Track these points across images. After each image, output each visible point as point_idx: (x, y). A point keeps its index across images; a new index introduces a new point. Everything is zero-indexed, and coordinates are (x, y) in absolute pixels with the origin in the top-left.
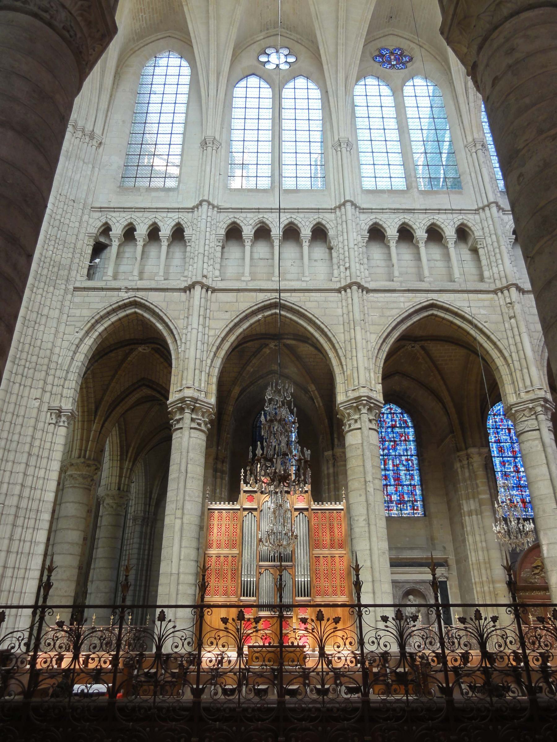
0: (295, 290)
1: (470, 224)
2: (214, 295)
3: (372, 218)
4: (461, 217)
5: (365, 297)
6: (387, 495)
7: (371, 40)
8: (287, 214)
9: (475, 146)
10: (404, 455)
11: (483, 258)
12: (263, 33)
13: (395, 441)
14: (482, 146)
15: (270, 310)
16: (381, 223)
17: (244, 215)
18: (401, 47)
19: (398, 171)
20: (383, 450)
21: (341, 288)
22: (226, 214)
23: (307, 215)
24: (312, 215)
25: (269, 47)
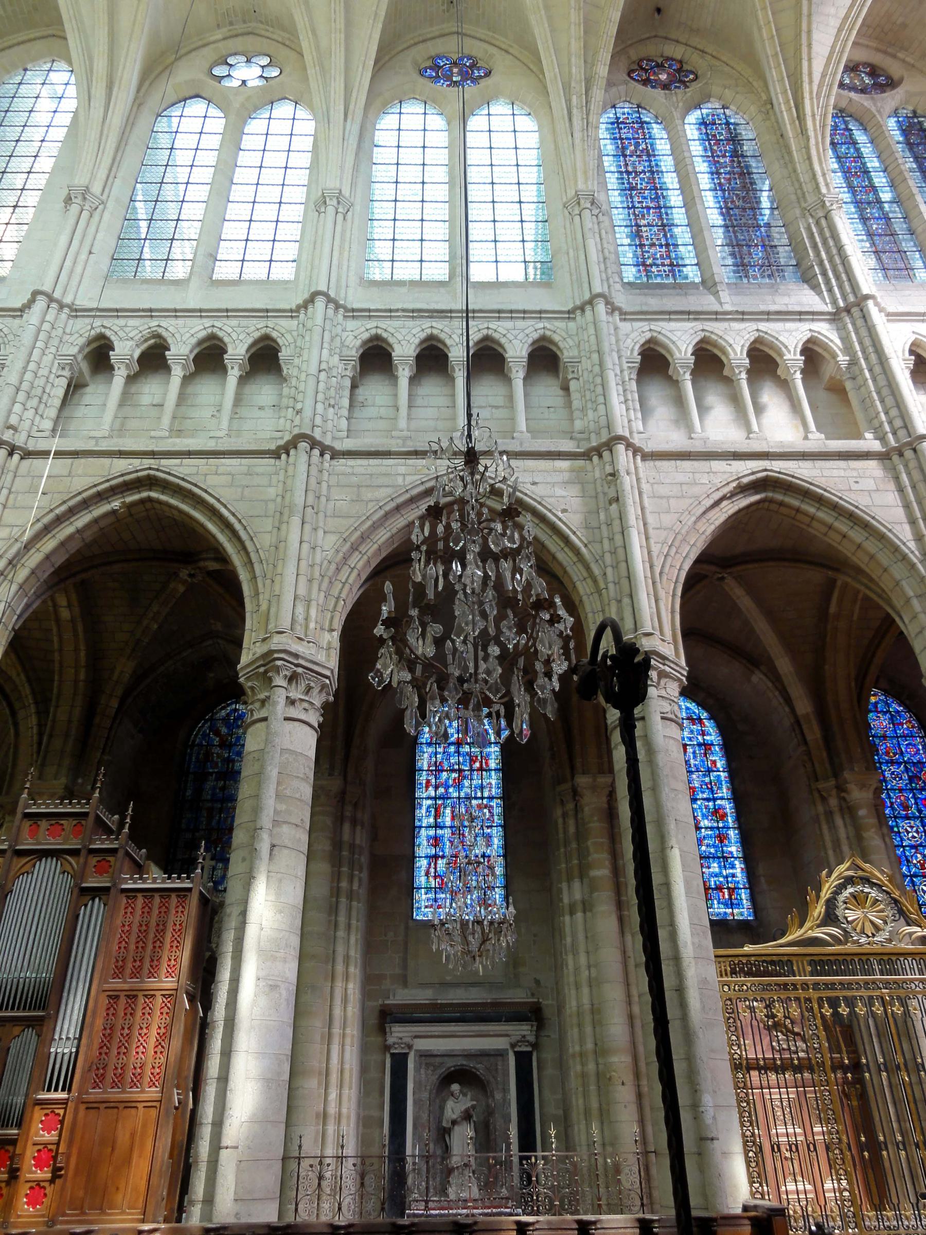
0: (189, 454)
1: (556, 338)
2: (26, 463)
3: (368, 327)
4: (541, 325)
5: (326, 465)
6: (435, 877)
7: (416, 40)
8: (205, 320)
9: (579, 203)
10: (476, 798)
11: (575, 396)
12: (225, 30)
13: (460, 771)
14: (593, 203)
15: (139, 492)
16: (385, 335)
17: (122, 322)
18: (474, 53)
19: (441, 251)
20: (436, 788)
21: (279, 447)
22: (87, 321)
23: (244, 322)
24: (254, 321)
25: (236, 54)
